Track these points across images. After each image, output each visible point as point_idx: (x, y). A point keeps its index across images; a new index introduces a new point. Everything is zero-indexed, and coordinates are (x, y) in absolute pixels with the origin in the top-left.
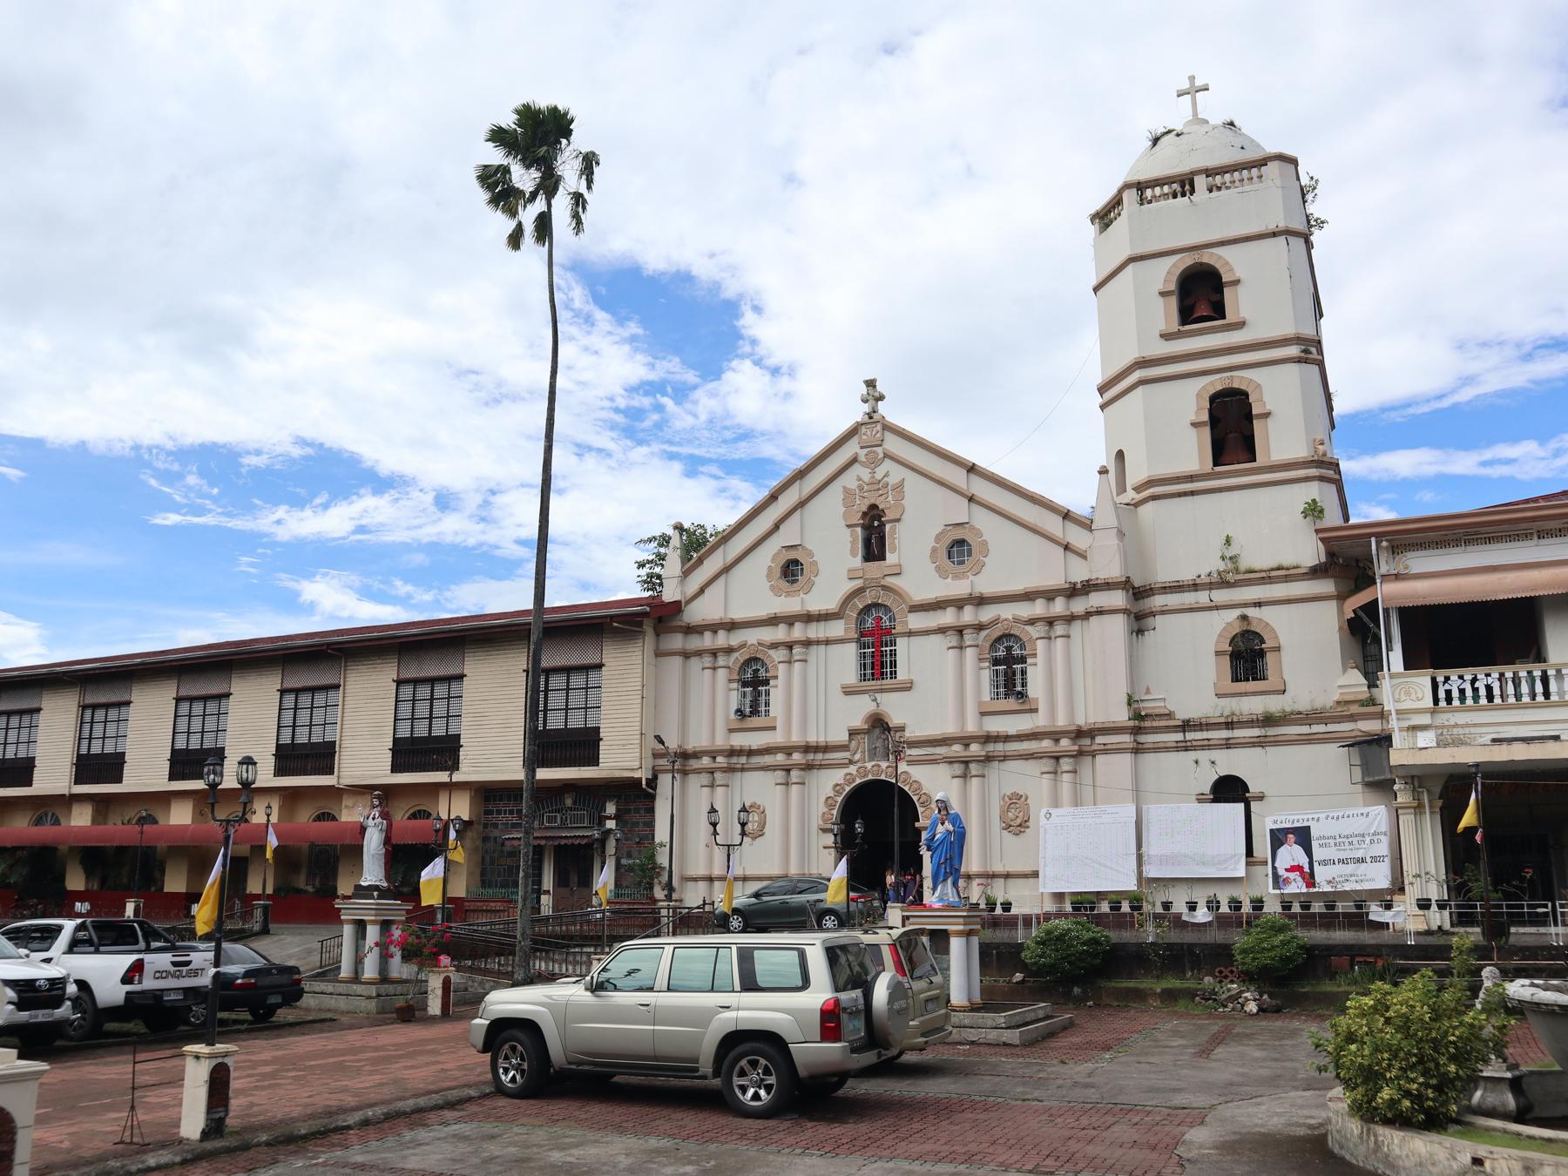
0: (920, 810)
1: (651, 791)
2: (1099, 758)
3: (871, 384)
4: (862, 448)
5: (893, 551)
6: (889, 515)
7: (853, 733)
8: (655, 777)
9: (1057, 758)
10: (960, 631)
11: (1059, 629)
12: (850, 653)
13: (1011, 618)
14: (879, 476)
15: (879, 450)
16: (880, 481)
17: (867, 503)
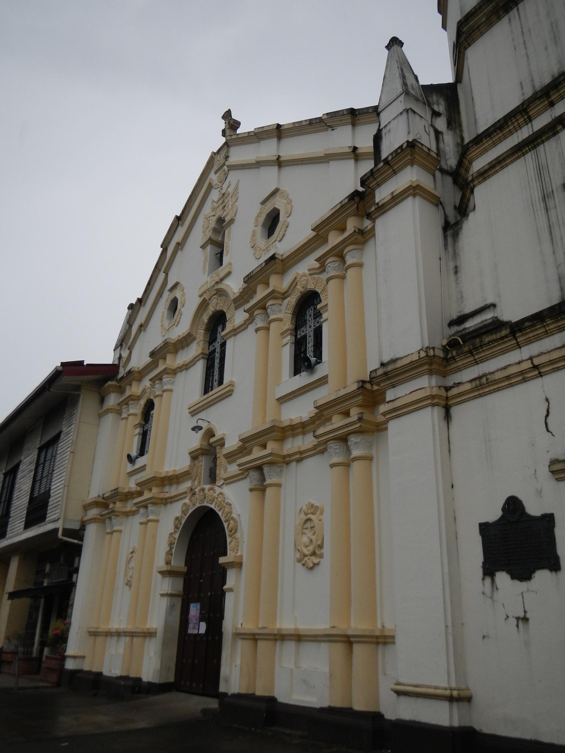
0: (229, 540)
1: (76, 541)
2: (393, 426)
3: (227, 115)
4: (216, 173)
5: (227, 254)
6: (227, 219)
7: (194, 456)
8: (83, 528)
9: (344, 439)
10: (262, 306)
11: (349, 260)
12: (199, 368)
13: (307, 272)
14: (223, 191)
15: (225, 168)
16: (224, 194)
17: (214, 219)
